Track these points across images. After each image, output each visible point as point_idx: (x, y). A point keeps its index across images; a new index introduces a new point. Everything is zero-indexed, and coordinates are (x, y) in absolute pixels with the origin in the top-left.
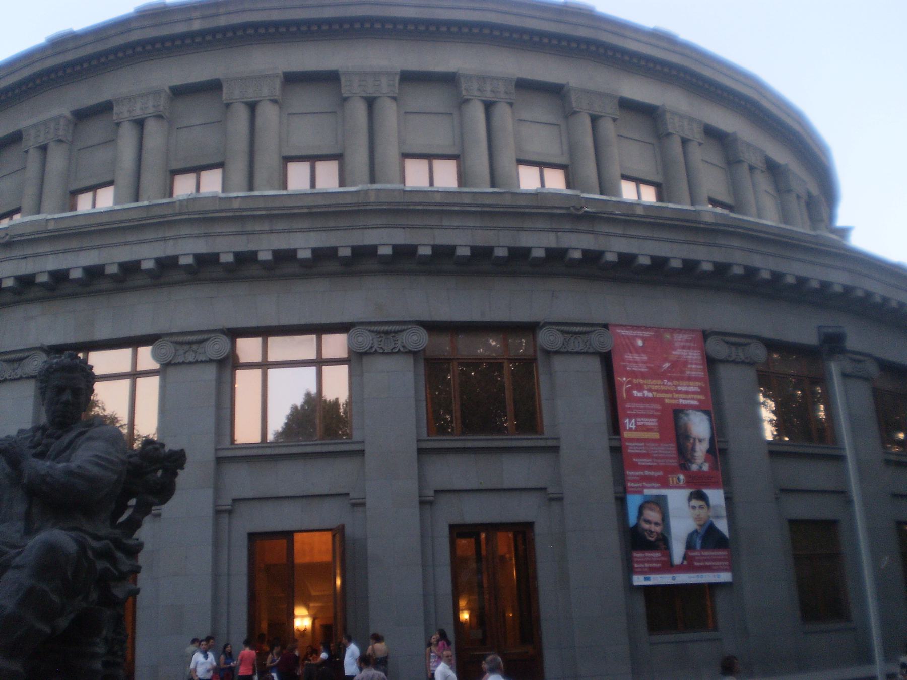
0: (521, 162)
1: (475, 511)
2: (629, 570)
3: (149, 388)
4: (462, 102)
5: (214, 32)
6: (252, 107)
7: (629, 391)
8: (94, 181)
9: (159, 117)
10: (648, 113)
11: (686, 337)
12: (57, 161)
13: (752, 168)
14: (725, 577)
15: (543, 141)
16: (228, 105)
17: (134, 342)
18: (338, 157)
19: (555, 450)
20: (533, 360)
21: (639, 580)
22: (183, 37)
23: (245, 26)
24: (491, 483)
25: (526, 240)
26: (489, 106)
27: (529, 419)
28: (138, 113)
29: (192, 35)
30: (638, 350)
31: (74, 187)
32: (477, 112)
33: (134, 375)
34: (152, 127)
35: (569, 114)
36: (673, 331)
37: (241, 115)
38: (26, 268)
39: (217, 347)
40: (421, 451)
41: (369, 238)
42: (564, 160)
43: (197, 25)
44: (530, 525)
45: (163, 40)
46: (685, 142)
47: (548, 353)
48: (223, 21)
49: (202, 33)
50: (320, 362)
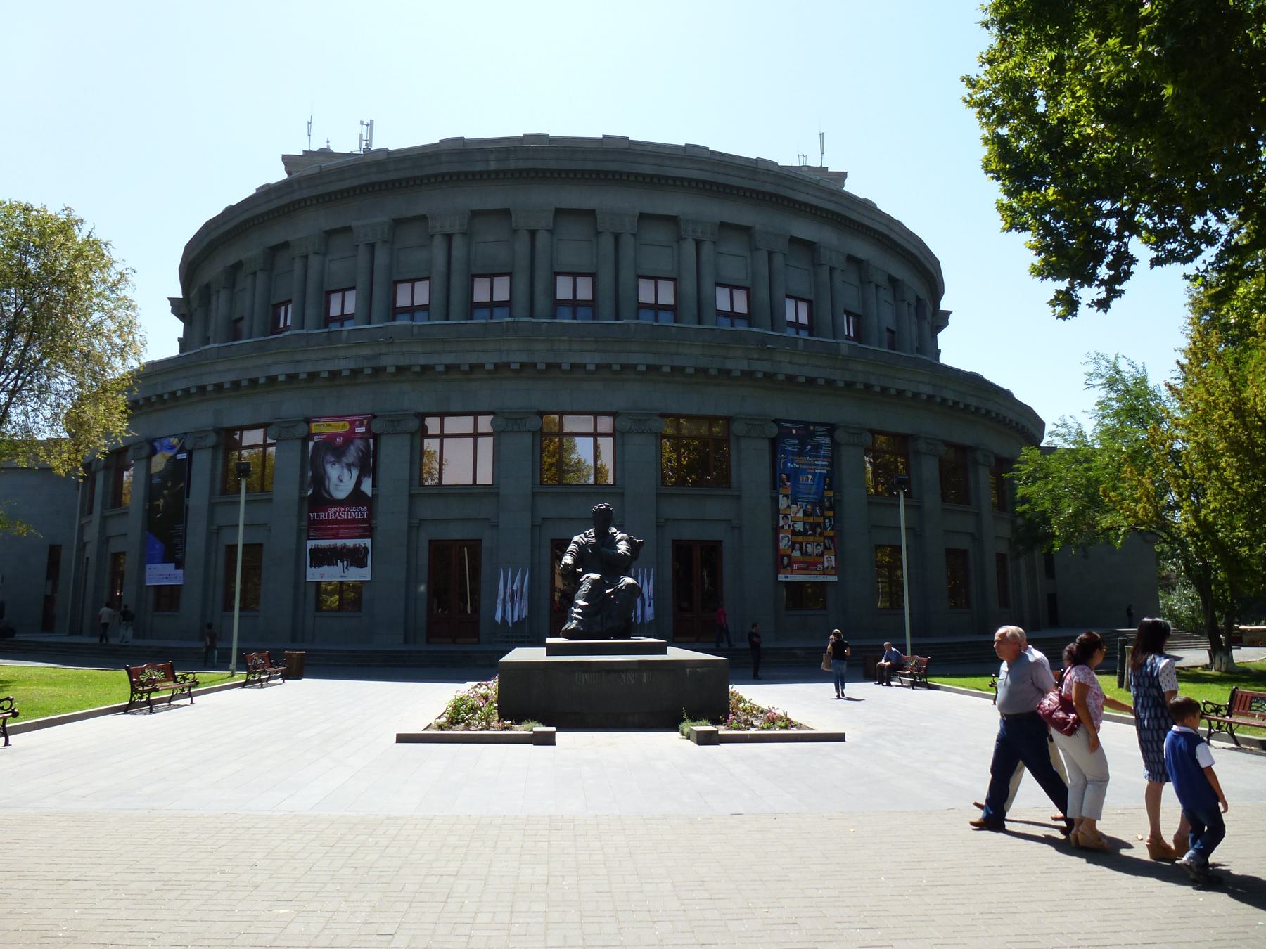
0: (718, 284)
1: (688, 533)
2: (777, 573)
3: (486, 445)
4: (680, 239)
5: (505, 172)
6: (533, 233)
7: (785, 464)
8: (413, 276)
9: (464, 234)
10: (810, 247)
11: (824, 428)
12: (381, 258)
13: (877, 286)
14: (834, 578)
15: (734, 268)
16: (515, 231)
17: (476, 414)
18: (592, 275)
19: (739, 497)
20: (726, 440)
21: (781, 578)
22: (481, 173)
23: (528, 171)
24: (701, 517)
25: (730, 365)
26: (698, 243)
27: (724, 480)
28: (448, 230)
29: (489, 173)
30: (794, 437)
31: (396, 278)
32: (689, 247)
33: (476, 435)
34: (458, 242)
35: (754, 249)
36: (815, 424)
37: (524, 239)
38: (403, 361)
39: (534, 423)
40: (658, 495)
41: (633, 359)
42: (747, 284)
43: (493, 166)
44: (720, 542)
45: (466, 174)
46: (832, 269)
47: (738, 438)
48: (512, 165)
49: (497, 172)
50: (595, 435)
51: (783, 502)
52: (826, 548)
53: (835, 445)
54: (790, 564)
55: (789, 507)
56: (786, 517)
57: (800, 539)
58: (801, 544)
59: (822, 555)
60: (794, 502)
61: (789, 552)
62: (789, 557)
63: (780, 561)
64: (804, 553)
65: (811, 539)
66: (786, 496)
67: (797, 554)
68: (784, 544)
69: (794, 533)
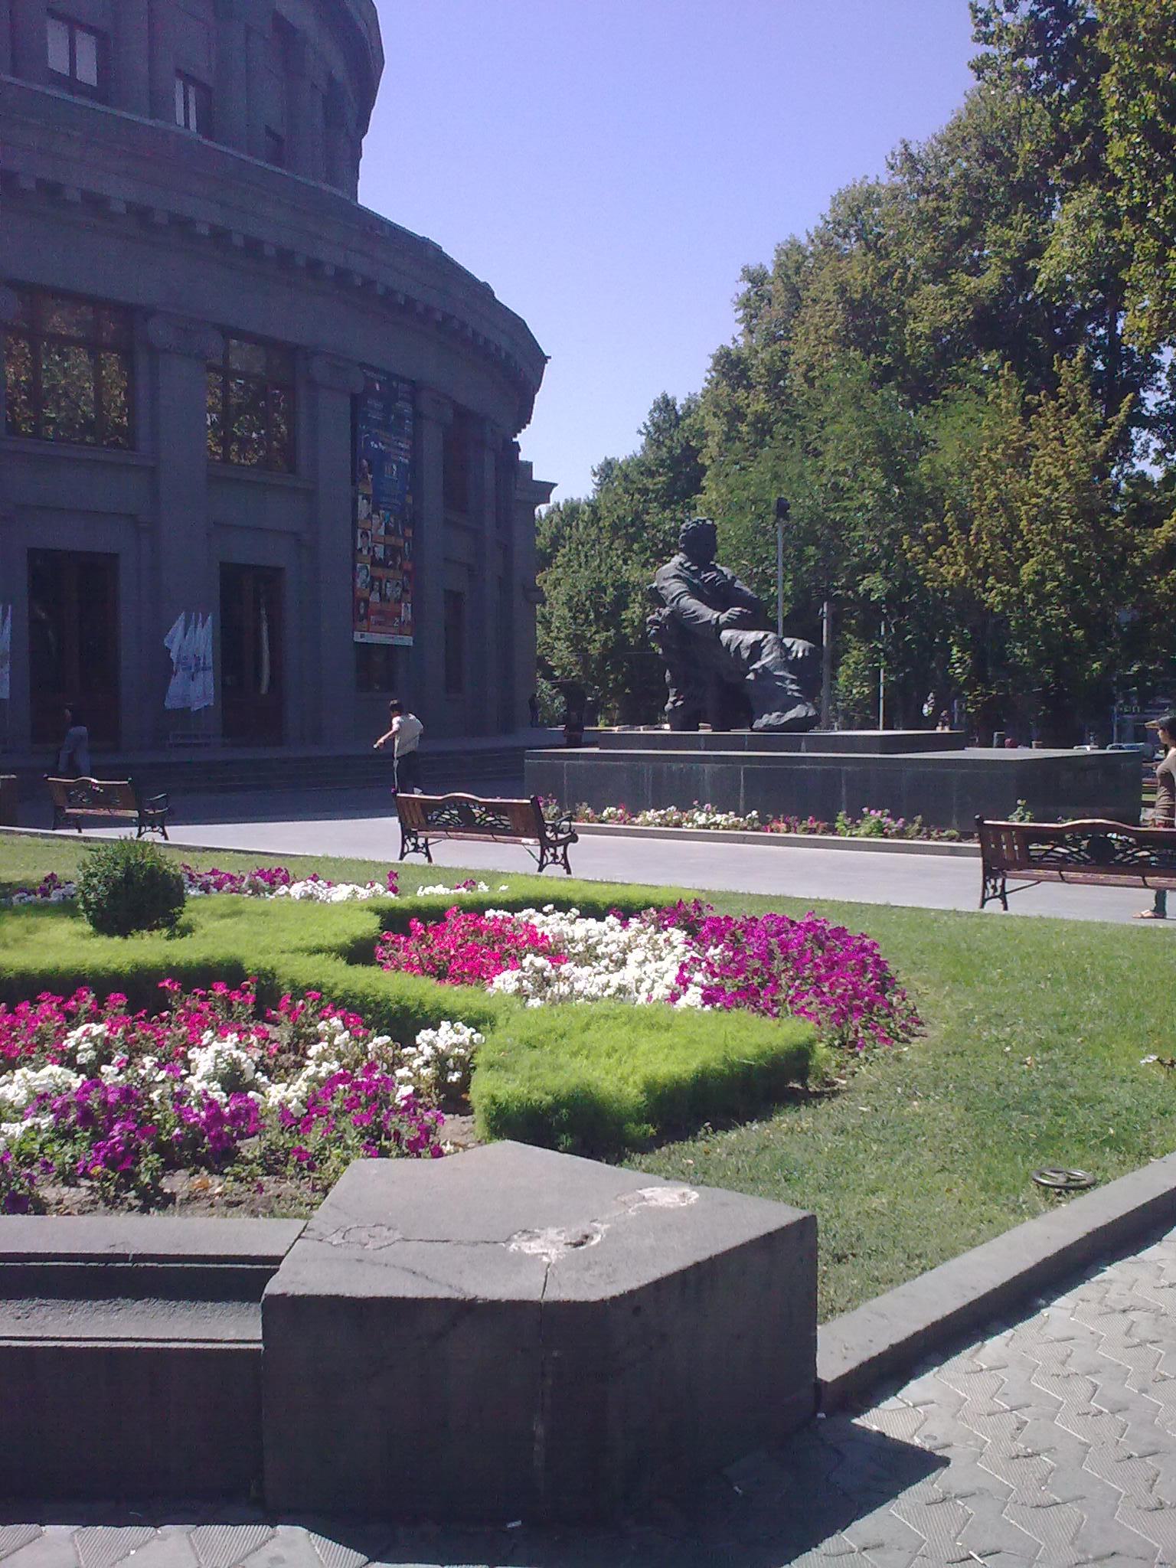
21: (357, 637)
44: (279, 570)
51: (363, 506)
52: (404, 590)
53: (417, 416)
54: (366, 616)
55: (369, 517)
56: (365, 534)
57: (379, 572)
58: (380, 580)
59: (399, 602)
60: (375, 511)
61: (366, 595)
62: (367, 601)
63: (359, 612)
64: (383, 597)
65: (391, 573)
66: (366, 497)
67: (375, 597)
68: (362, 577)
69: (375, 562)
